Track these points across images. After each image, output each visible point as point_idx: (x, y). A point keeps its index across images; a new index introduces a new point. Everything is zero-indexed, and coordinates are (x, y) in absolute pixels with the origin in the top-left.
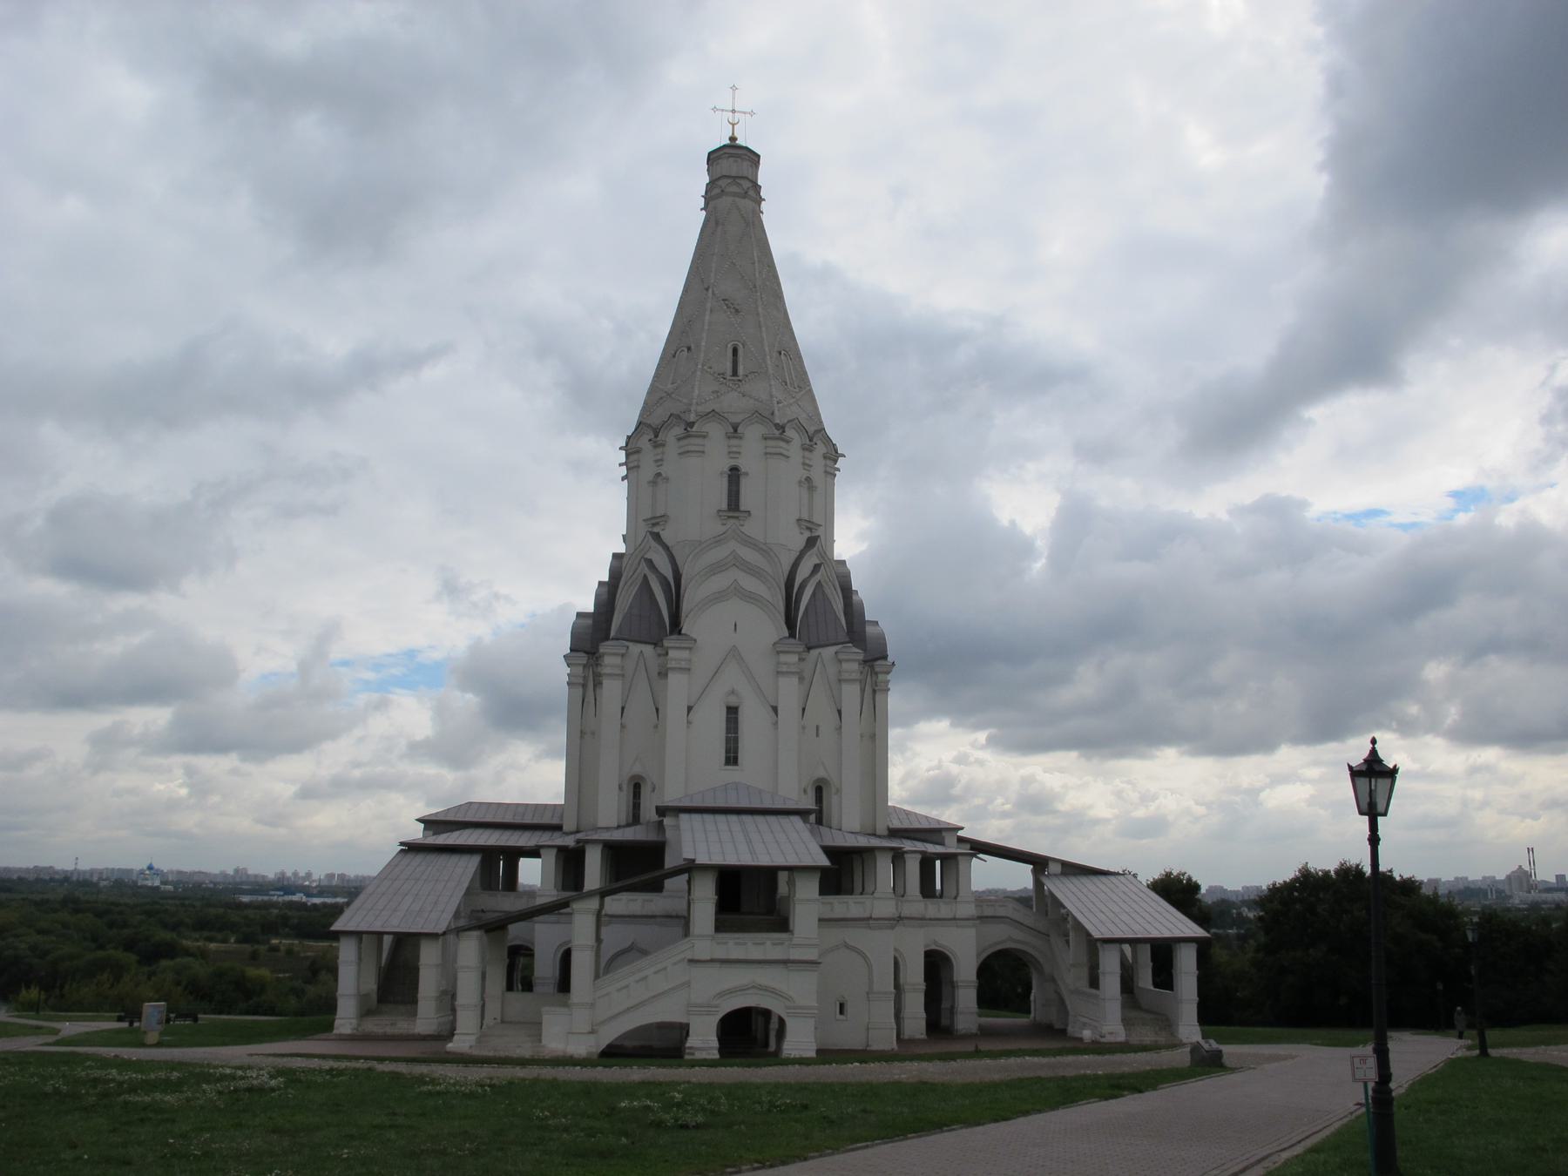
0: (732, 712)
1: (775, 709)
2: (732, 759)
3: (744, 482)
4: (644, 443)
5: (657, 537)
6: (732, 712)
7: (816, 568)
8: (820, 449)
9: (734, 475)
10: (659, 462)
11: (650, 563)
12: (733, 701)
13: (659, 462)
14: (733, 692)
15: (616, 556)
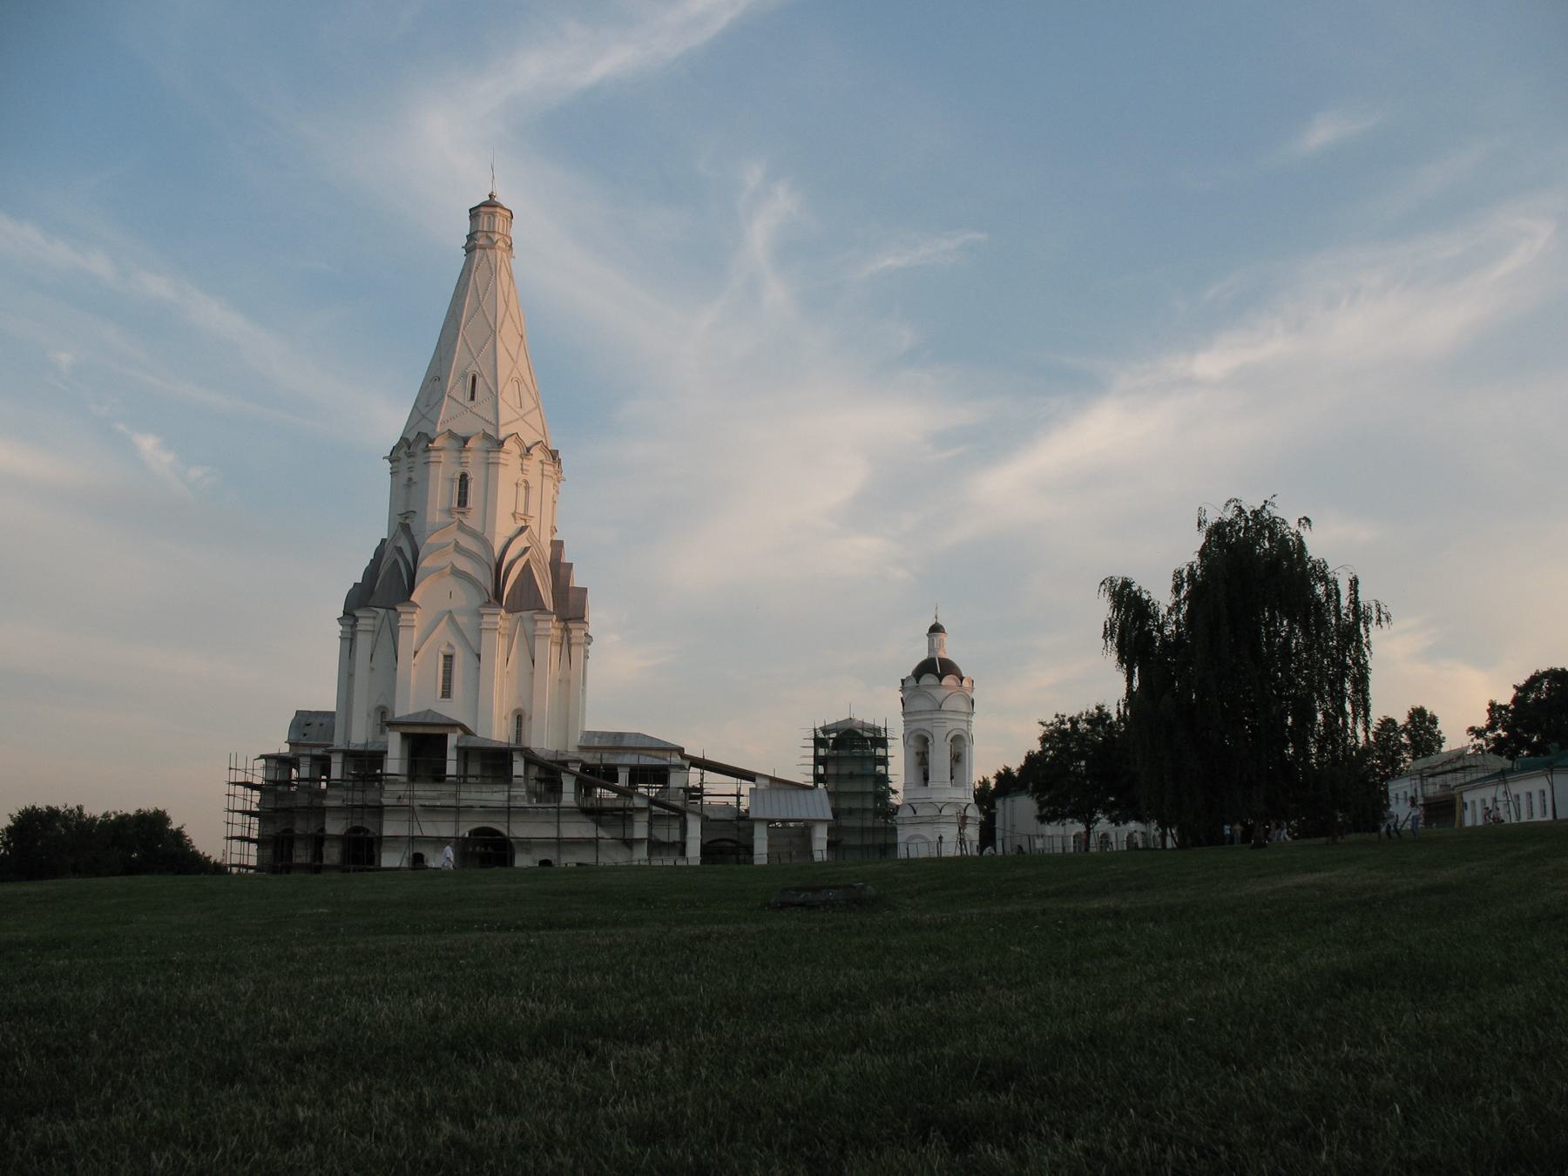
0: (449, 659)
1: (479, 656)
2: (447, 693)
3: (472, 487)
4: (402, 454)
5: (406, 528)
6: (449, 659)
7: (526, 550)
8: (537, 454)
9: (464, 479)
10: (410, 469)
11: (400, 550)
12: (449, 652)
13: (410, 469)
14: (449, 645)
15: (383, 541)
